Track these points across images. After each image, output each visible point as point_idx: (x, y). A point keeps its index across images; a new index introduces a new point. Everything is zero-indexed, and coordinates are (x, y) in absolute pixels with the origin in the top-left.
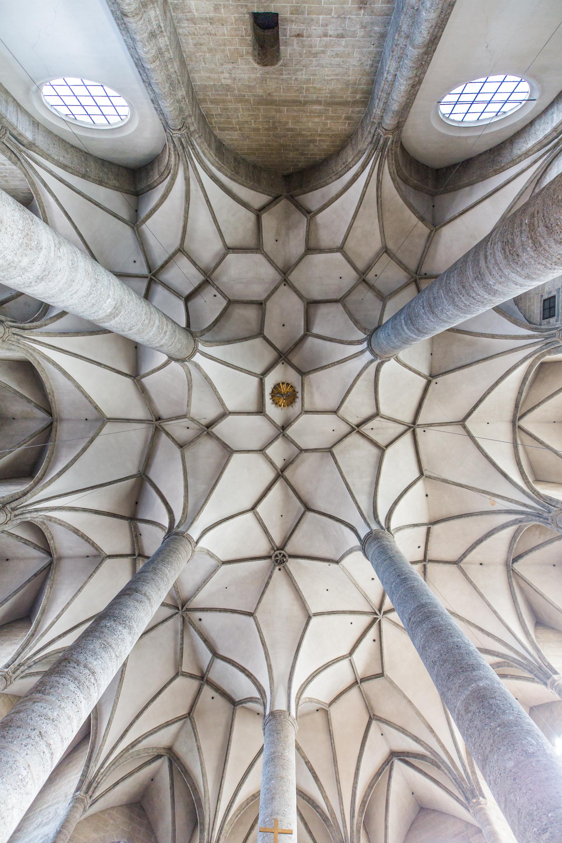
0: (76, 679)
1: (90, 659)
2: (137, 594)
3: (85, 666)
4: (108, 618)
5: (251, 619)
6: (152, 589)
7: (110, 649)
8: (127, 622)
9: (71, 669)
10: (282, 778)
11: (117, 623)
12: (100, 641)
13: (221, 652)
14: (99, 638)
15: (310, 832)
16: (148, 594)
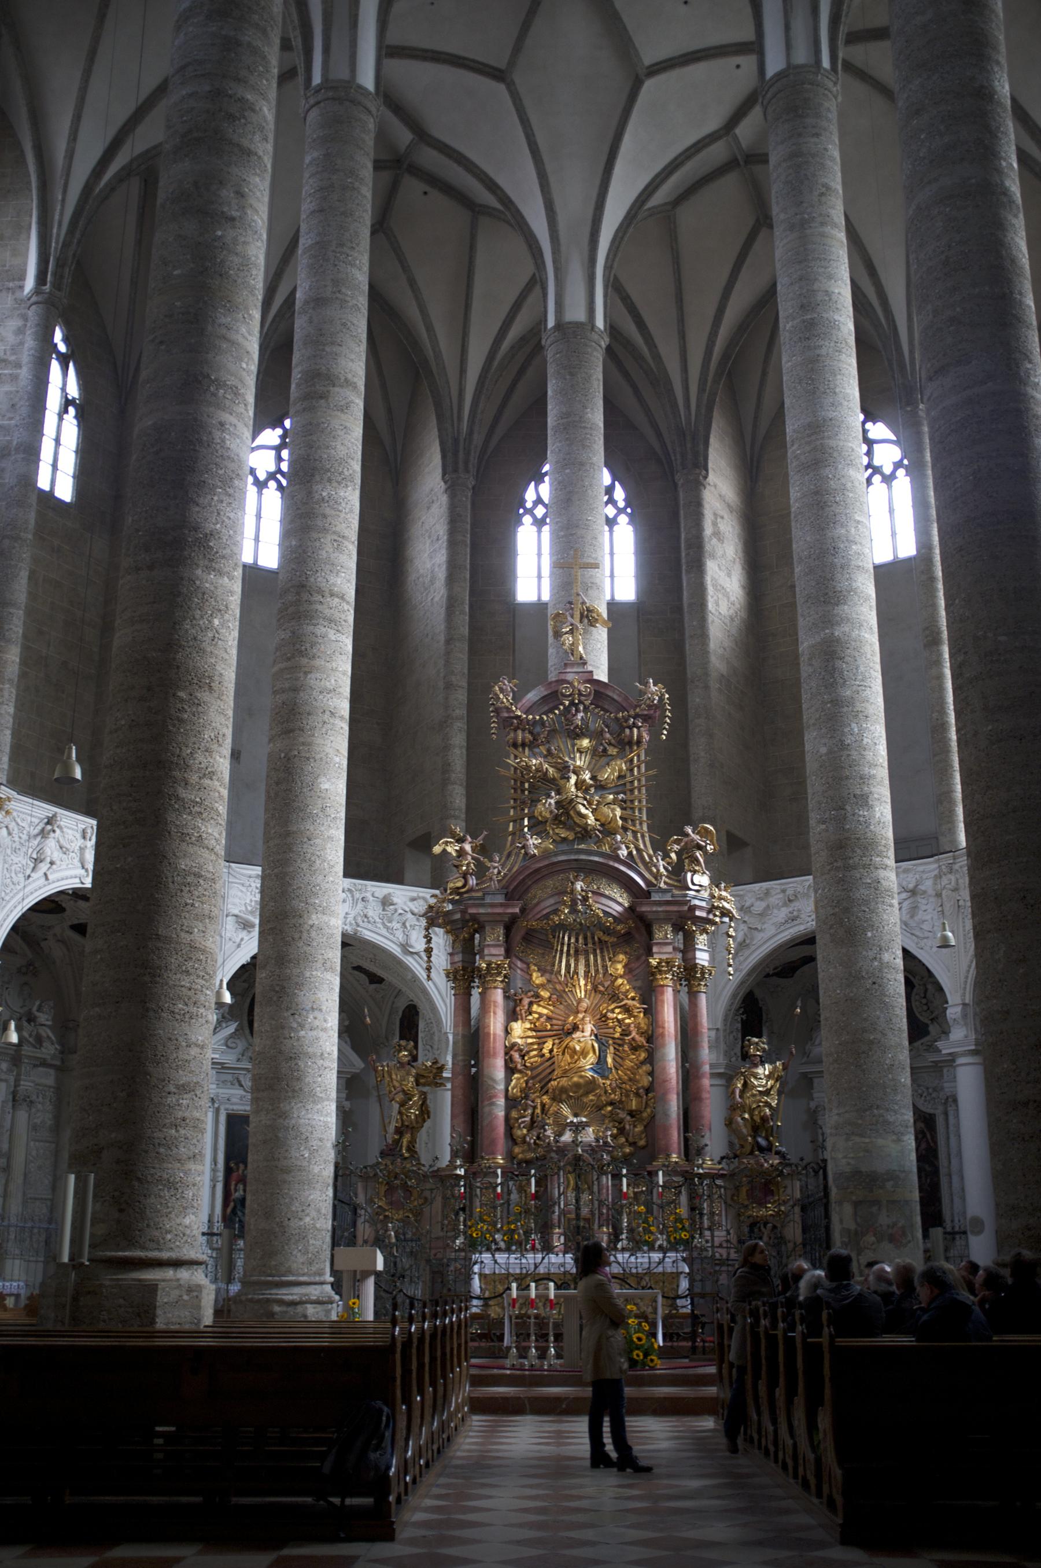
0: (331, 621)
1: (332, 579)
2: (337, 389)
3: (332, 595)
4: (317, 478)
5: (502, 87)
6: (353, 357)
7: (346, 543)
8: (346, 473)
9: (319, 607)
10: (582, 464)
11: (335, 484)
12: (329, 537)
13: (438, 132)
14: (325, 530)
15: (626, 375)
16: (349, 376)
